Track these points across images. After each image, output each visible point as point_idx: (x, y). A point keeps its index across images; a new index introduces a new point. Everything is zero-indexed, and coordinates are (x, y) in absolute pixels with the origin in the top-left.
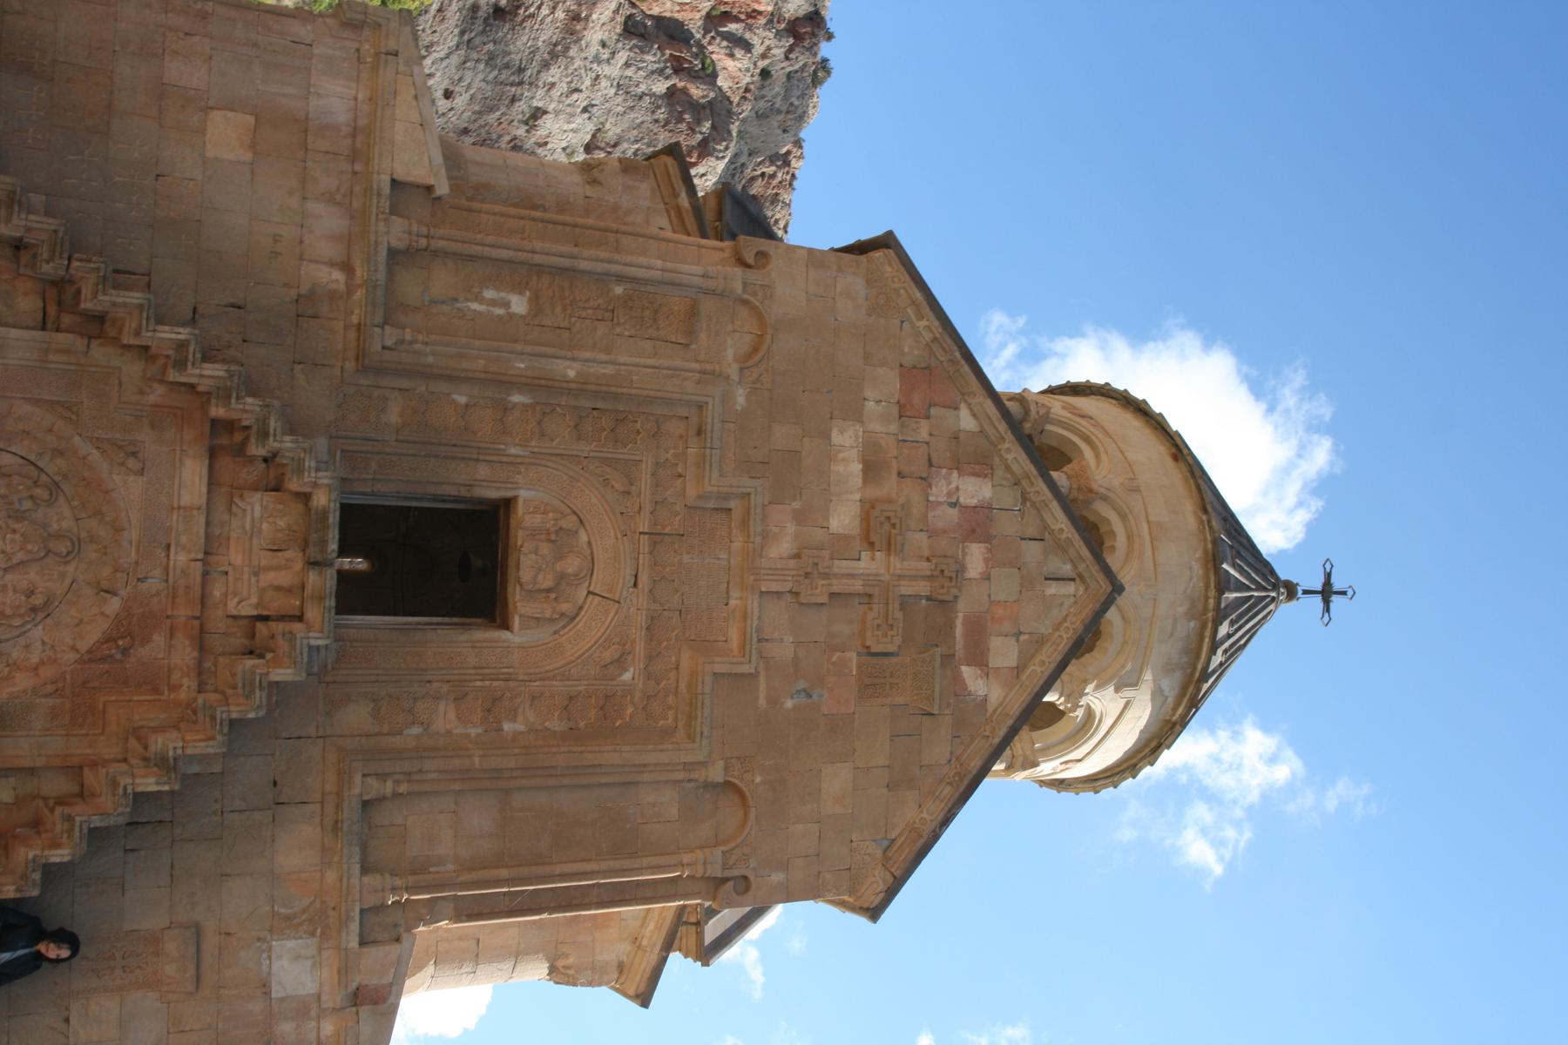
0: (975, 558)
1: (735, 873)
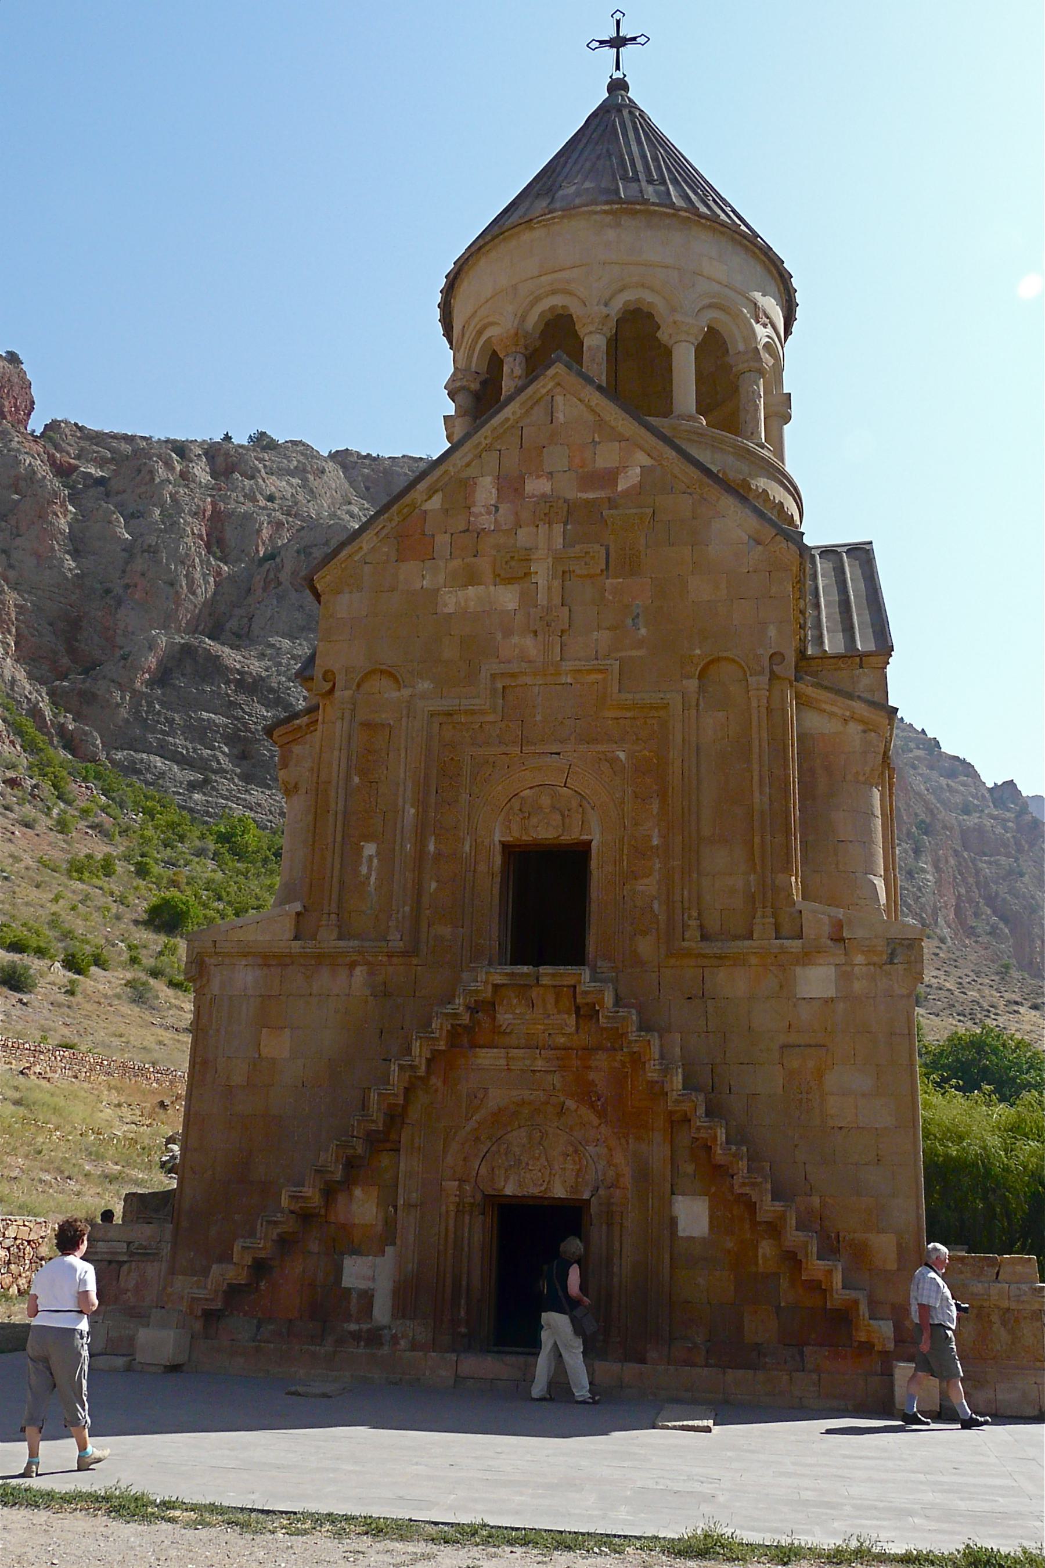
0: (536, 486)
1: (767, 664)
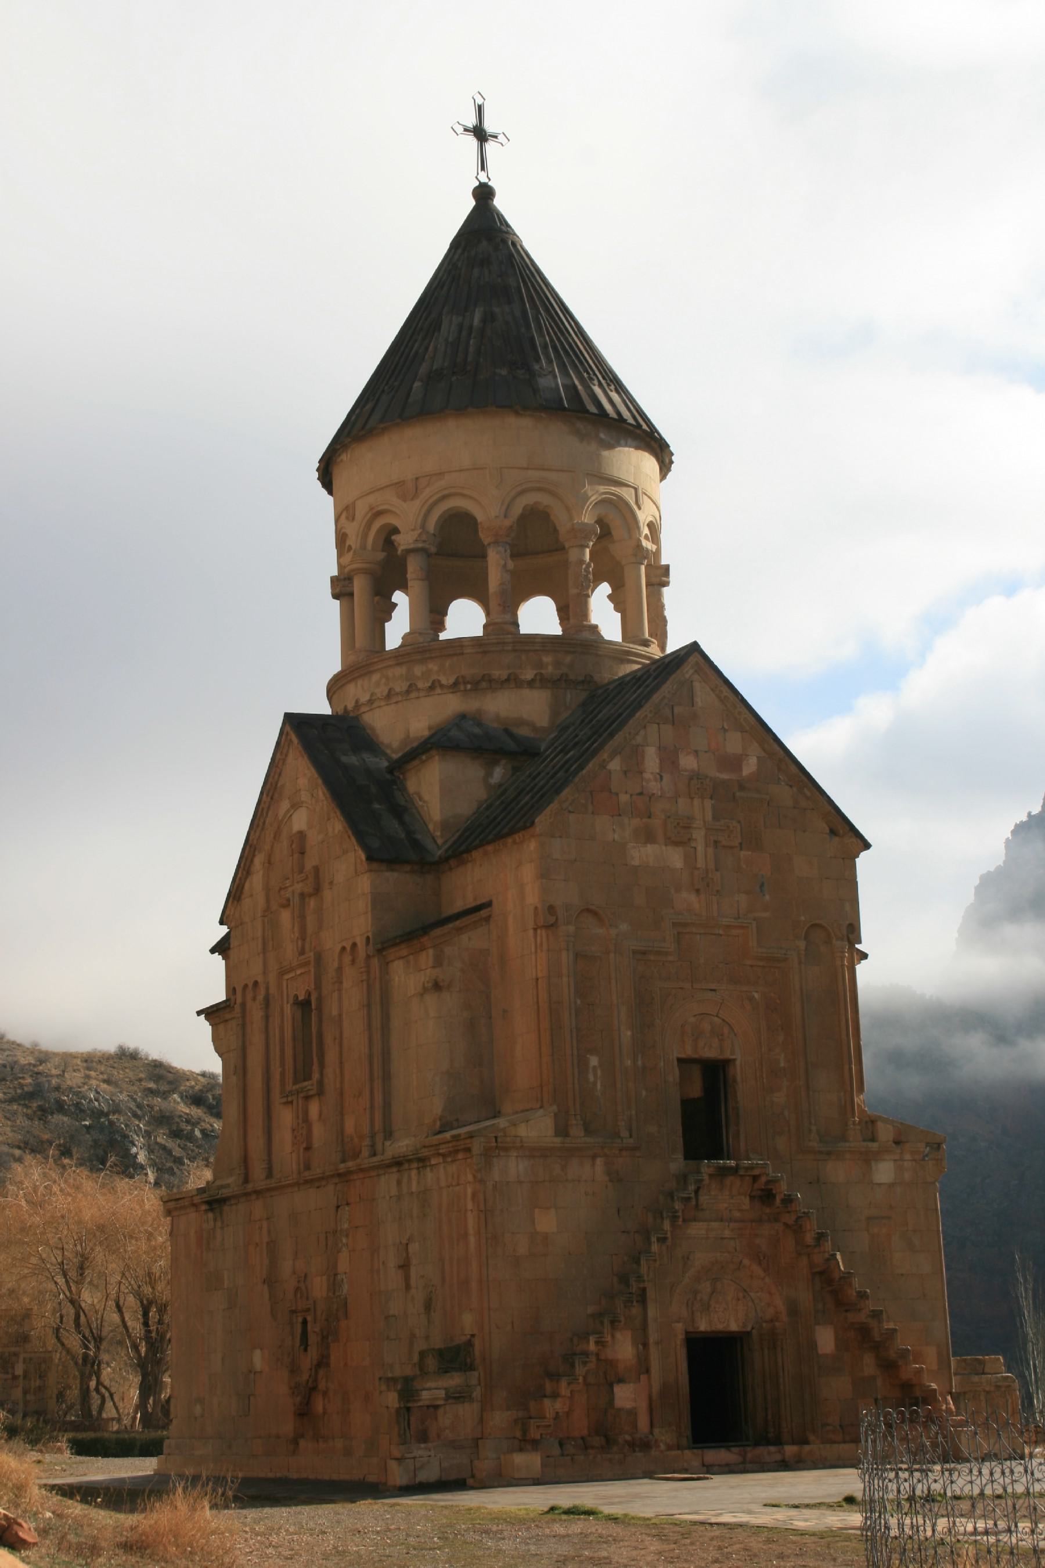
0: (688, 762)
